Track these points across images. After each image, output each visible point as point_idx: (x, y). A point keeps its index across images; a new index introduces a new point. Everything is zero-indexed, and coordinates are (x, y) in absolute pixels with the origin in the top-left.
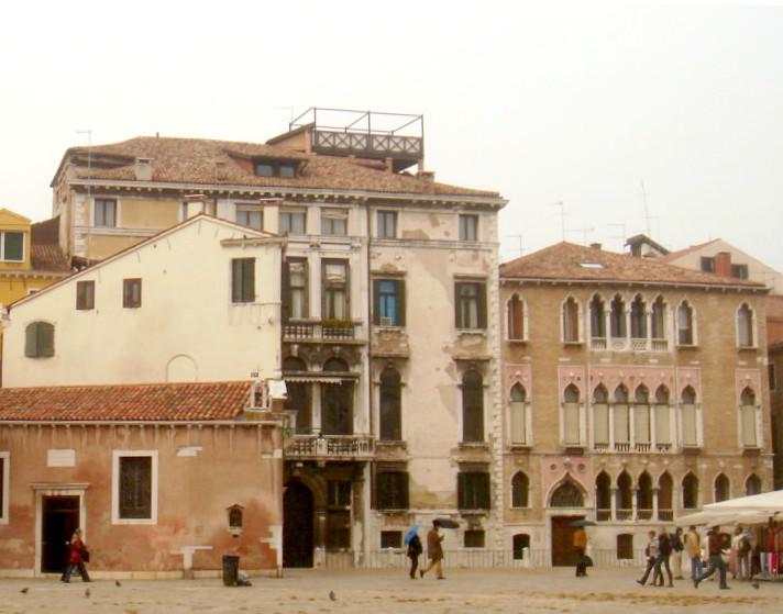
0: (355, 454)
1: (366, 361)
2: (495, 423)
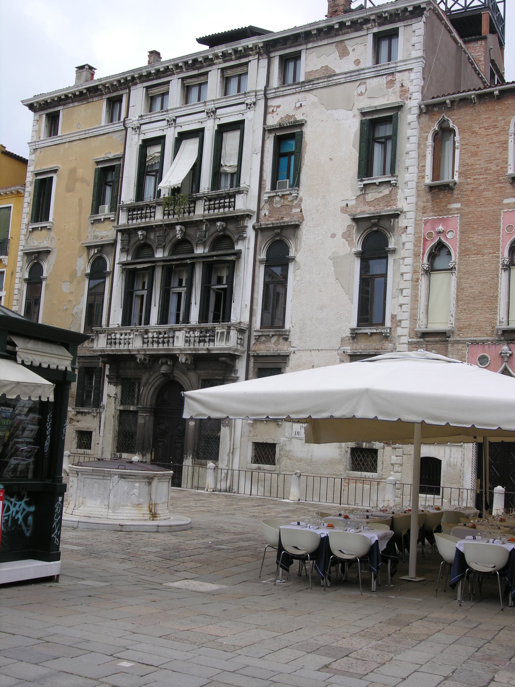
0: (211, 346)
1: (250, 234)
2: (402, 300)
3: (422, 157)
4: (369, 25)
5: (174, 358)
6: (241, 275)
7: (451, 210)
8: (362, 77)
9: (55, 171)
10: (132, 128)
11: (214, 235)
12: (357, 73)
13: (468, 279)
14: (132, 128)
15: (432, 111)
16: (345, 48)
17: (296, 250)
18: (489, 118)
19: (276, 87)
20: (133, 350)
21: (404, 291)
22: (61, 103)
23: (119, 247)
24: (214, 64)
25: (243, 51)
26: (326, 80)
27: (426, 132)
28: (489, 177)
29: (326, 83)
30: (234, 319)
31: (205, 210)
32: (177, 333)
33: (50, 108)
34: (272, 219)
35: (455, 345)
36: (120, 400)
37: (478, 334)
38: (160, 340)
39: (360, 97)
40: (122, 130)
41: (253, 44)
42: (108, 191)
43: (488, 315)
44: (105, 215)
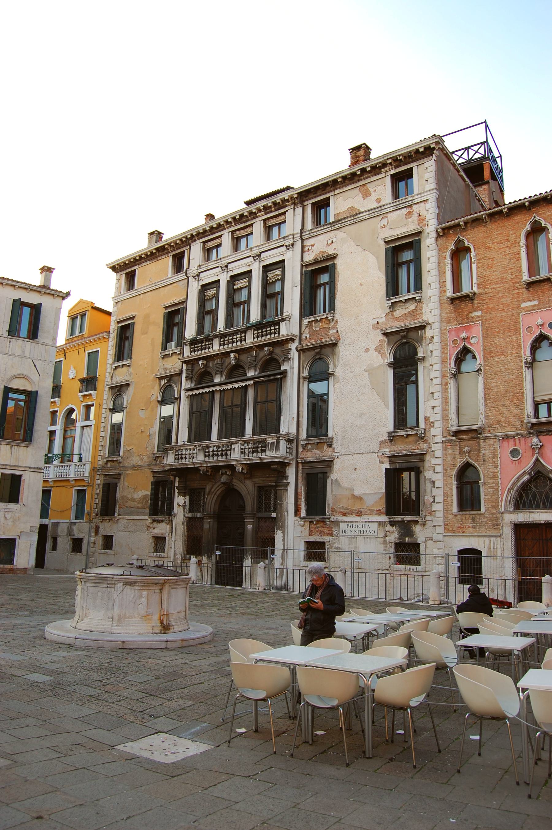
0: (263, 455)
1: (294, 355)
2: (433, 403)
3: (442, 273)
4: (387, 169)
5: (232, 468)
6: (288, 391)
7: (473, 318)
8: (384, 212)
9: (133, 318)
10: (193, 276)
11: (263, 359)
12: (379, 209)
13: (494, 378)
14: (193, 276)
15: (448, 233)
16: (367, 189)
17: (335, 366)
18: (500, 234)
19: (310, 229)
20: (197, 463)
21: (435, 394)
22: (136, 263)
23: (184, 375)
24: (257, 217)
25: (281, 203)
26: (352, 218)
27: (444, 252)
28: (506, 286)
29: (352, 221)
30: (284, 430)
31: (254, 338)
32: (233, 446)
33: (129, 268)
34: (312, 341)
35: (487, 441)
36: (188, 508)
37: (508, 429)
38: (219, 453)
39: (383, 229)
40: (185, 279)
41: (289, 196)
42: (176, 330)
43: (516, 411)
44: (172, 350)
